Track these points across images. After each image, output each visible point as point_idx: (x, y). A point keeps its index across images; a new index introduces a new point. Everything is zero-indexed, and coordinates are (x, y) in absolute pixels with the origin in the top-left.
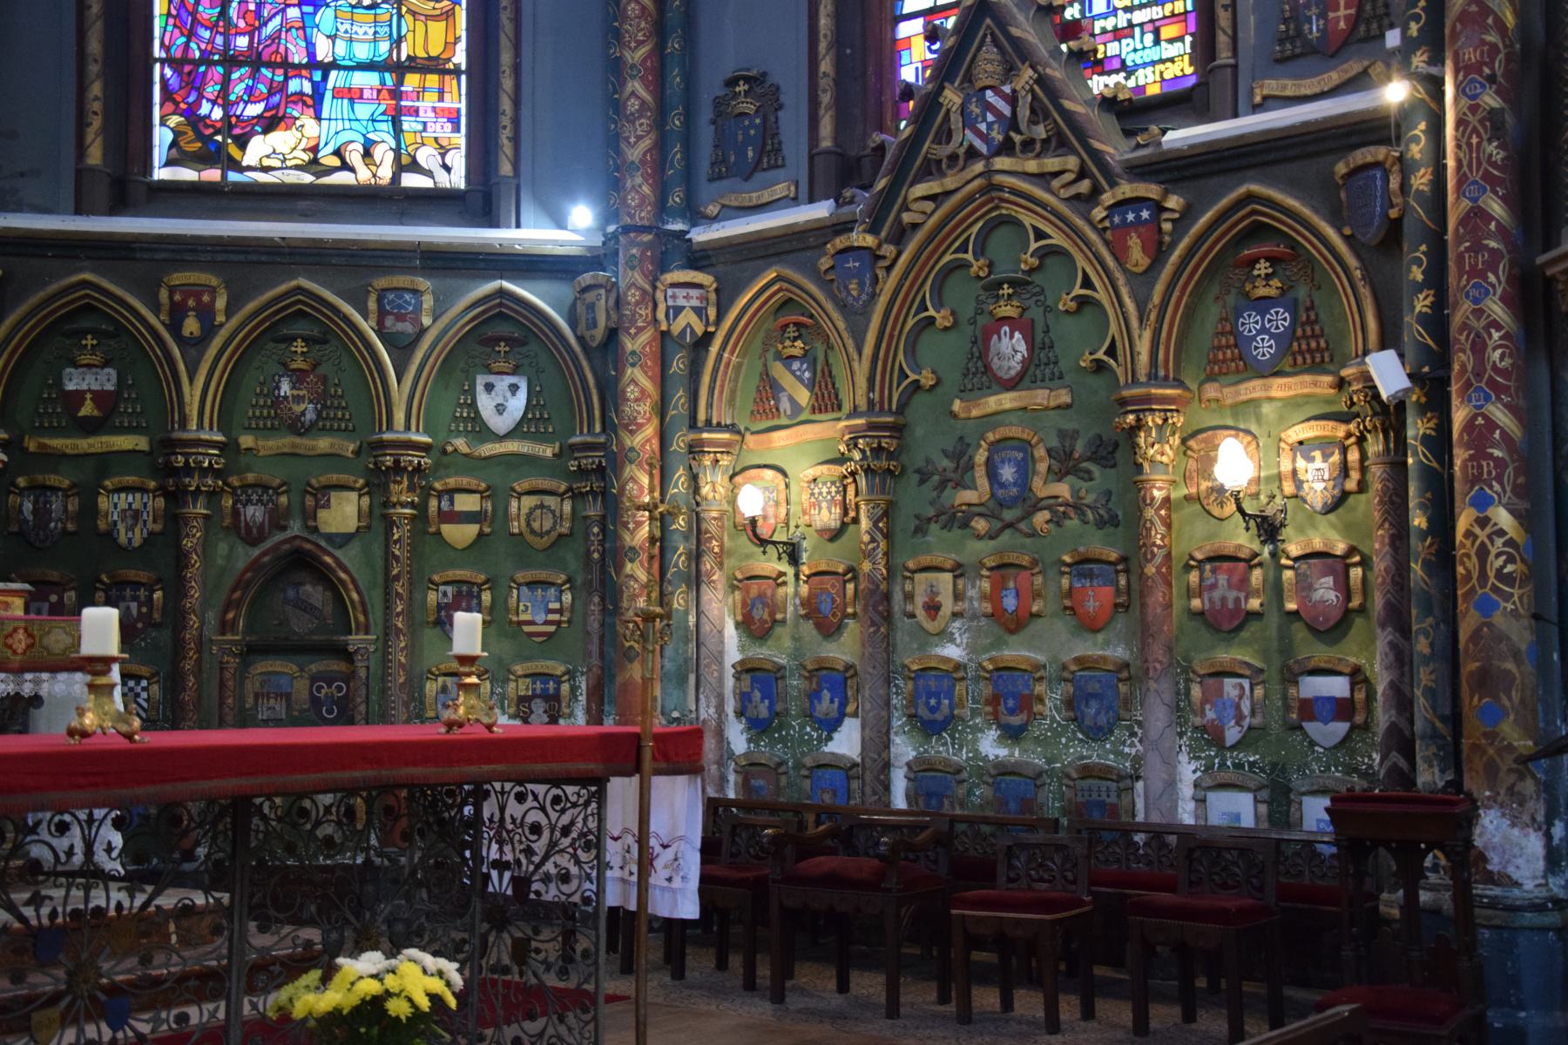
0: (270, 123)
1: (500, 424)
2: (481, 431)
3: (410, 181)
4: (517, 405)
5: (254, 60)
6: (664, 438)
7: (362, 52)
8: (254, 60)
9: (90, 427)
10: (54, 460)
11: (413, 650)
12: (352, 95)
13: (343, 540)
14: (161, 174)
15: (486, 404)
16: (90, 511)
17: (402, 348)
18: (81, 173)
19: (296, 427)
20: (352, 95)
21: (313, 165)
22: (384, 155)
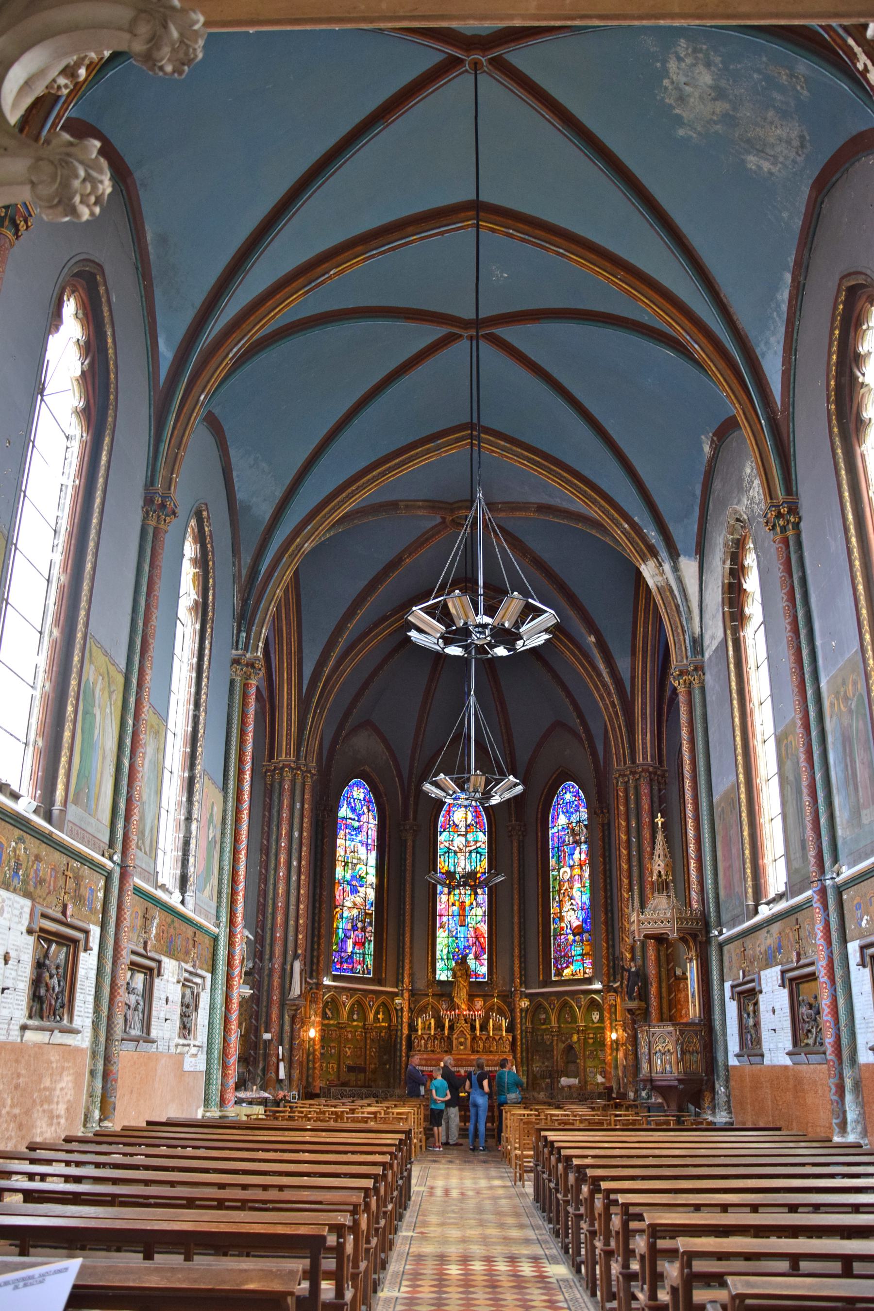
0: (567, 967)
1: (596, 1021)
2: (593, 1022)
3: (586, 976)
4: (598, 1017)
5: (564, 956)
6: (611, 1024)
7: (578, 953)
8: (564, 956)
9: (543, 1024)
10: (538, 1029)
11: (585, 1062)
12: (577, 961)
13: (576, 1043)
14: (553, 979)
15: (594, 1017)
16: (543, 1039)
17: (579, 1008)
18: (539, 982)
19: (568, 1022)
20: (577, 961)
21: (572, 975)
22: (582, 971)
